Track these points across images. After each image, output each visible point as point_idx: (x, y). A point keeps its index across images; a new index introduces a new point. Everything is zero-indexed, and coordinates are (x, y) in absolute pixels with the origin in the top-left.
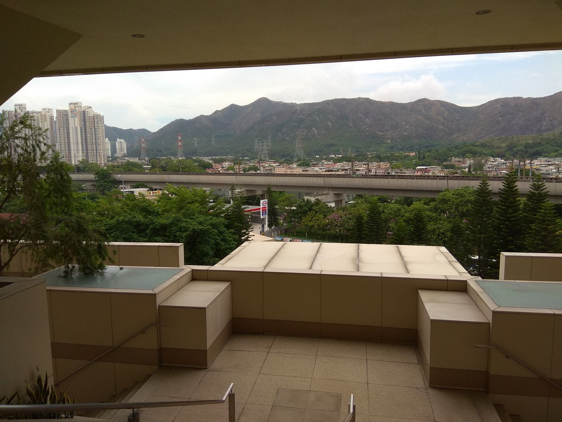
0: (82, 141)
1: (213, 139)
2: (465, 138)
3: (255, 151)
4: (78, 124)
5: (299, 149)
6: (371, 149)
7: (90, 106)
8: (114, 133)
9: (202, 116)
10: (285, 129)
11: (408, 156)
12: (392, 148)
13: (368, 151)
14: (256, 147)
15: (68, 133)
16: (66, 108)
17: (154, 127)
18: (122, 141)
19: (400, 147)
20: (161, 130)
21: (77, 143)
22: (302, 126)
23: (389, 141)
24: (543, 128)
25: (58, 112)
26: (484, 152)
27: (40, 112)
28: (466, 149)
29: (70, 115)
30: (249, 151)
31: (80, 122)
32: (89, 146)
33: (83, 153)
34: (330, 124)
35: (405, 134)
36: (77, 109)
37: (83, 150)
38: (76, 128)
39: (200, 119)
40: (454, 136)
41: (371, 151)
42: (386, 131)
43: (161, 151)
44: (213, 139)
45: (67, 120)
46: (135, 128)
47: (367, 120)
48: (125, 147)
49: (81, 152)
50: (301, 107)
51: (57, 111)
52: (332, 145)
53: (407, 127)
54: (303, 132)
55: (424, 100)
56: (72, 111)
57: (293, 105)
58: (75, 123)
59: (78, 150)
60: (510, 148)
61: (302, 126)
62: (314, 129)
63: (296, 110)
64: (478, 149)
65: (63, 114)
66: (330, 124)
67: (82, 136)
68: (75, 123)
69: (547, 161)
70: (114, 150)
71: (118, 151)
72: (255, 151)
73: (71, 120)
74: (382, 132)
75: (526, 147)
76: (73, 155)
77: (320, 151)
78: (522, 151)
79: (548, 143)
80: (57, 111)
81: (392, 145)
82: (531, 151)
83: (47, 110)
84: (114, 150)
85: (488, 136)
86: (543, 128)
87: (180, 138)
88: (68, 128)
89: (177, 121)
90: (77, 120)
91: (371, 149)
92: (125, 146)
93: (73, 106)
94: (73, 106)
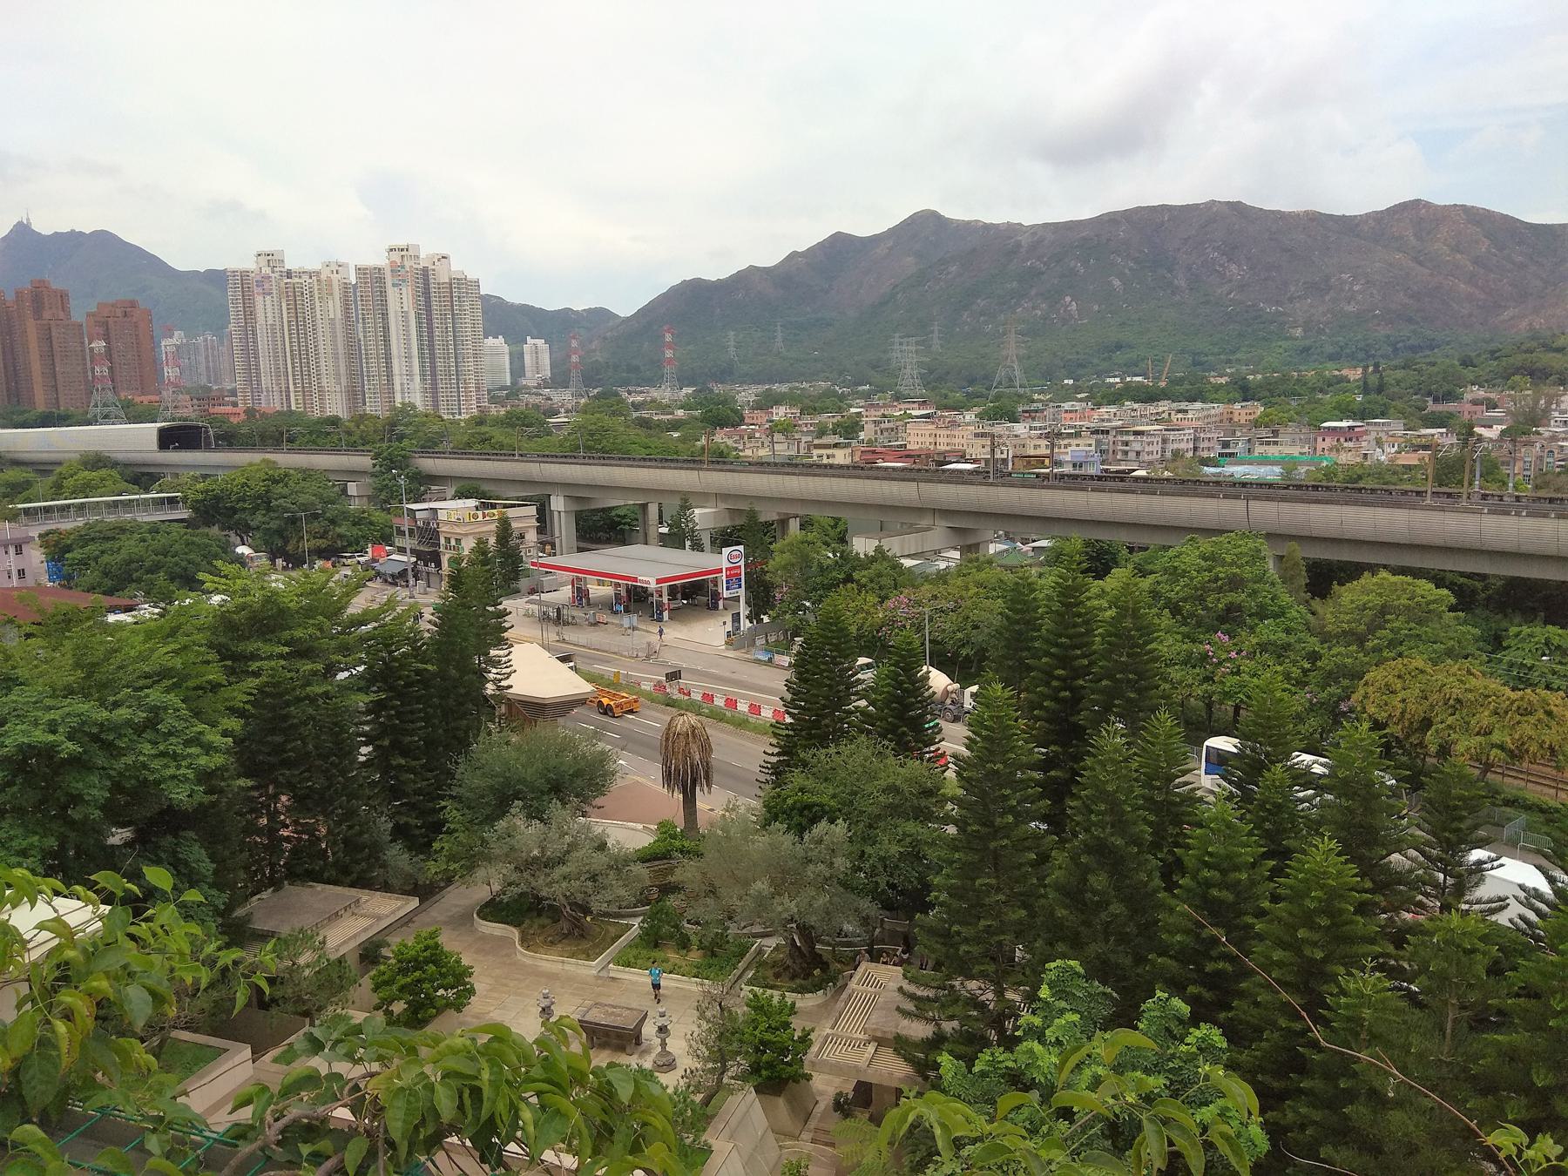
0: (421, 349)
1: (779, 335)
2: (1539, 323)
4: (409, 305)
5: (1011, 359)
6: (1238, 356)
7: (444, 252)
8: (512, 321)
9: (752, 270)
10: (981, 302)
13: (1229, 361)
15: (386, 329)
16: (379, 259)
17: (625, 306)
18: (540, 342)
19: (1329, 349)
20: (643, 312)
21: (409, 357)
22: (1033, 292)
23: (1299, 332)
25: (360, 270)
27: (318, 273)
29: (389, 281)
31: (416, 297)
32: (439, 364)
33: (423, 380)
34: (1117, 283)
35: (1350, 308)
36: (407, 264)
37: (423, 375)
38: (405, 315)
39: (746, 279)
40: (1506, 315)
41: (1238, 361)
42: (1291, 300)
43: (637, 369)
44: (779, 335)
45: (383, 293)
46: (579, 306)
47: (1233, 267)
48: (547, 362)
49: (417, 378)
51: (358, 269)
52: (1119, 347)
53: (1356, 288)
54: (1034, 308)
56: (396, 269)
58: (401, 302)
59: (410, 375)
61: (1033, 292)
62: (1068, 299)
65: (373, 279)
66: (1117, 283)
67: (420, 336)
68: (401, 302)
70: (518, 369)
71: (528, 374)
73: (392, 294)
74: (1278, 303)
76: (397, 387)
77: (1084, 366)
80: (358, 269)
81: (1307, 343)
83: (334, 268)
84: (518, 369)
87: (668, 338)
88: (385, 315)
90: (408, 293)
92: (546, 360)
93: (396, 257)
94: (396, 257)
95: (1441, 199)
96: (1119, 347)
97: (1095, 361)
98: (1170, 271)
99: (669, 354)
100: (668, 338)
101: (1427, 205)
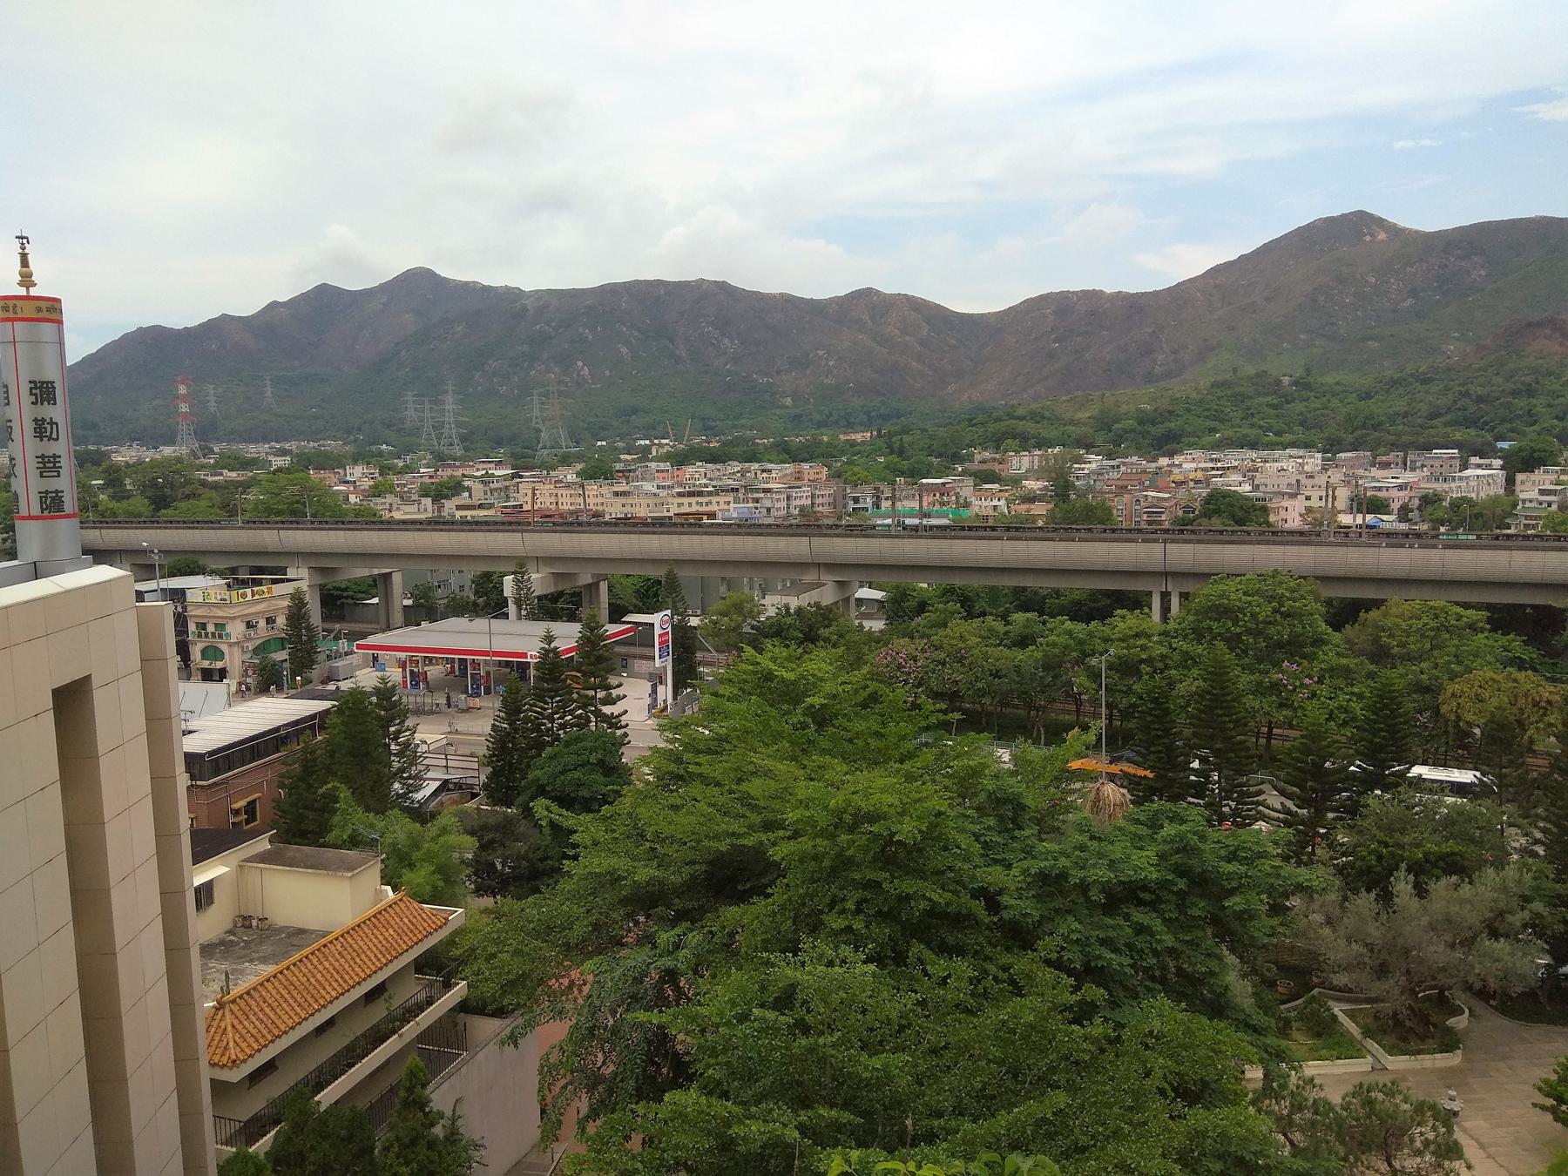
1: (269, 390)
3: (408, 424)
6: (743, 421)
11: (853, 444)
12: (797, 419)
13: (734, 426)
14: (410, 413)
22: (545, 355)
23: (788, 401)
24: (1158, 370)
26: (1044, 433)
28: (1002, 426)
30: (389, 426)
34: (624, 350)
35: (828, 381)
42: (778, 372)
44: (269, 390)
47: (726, 341)
50: (539, 299)
55: (868, 292)
57: (510, 296)
60: (1105, 423)
61: (545, 355)
62: (580, 363)
63: (525, 309)
64: (1029, 427)
66: (624, 350)
69: (1211, 460)
72: (408, 424)
74: (767, 375)
75: (1141, 422)
77: (602, 428)
78: (1133, 431)
79: (1188, 410)
81: (798, 411)
82: (1157, 431)
85: (1031, 391)
86: (1158, 370)
89: (142, 332)
91: (743, 421)
95: (888, 288)
96: (635, 411)
97: (615, 424)
98: (672, 342)
99: (184, 408)
100: (182, 390)
101: (878, 292)
